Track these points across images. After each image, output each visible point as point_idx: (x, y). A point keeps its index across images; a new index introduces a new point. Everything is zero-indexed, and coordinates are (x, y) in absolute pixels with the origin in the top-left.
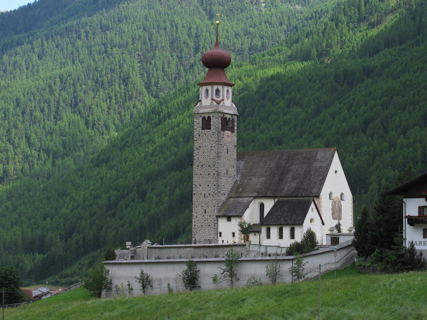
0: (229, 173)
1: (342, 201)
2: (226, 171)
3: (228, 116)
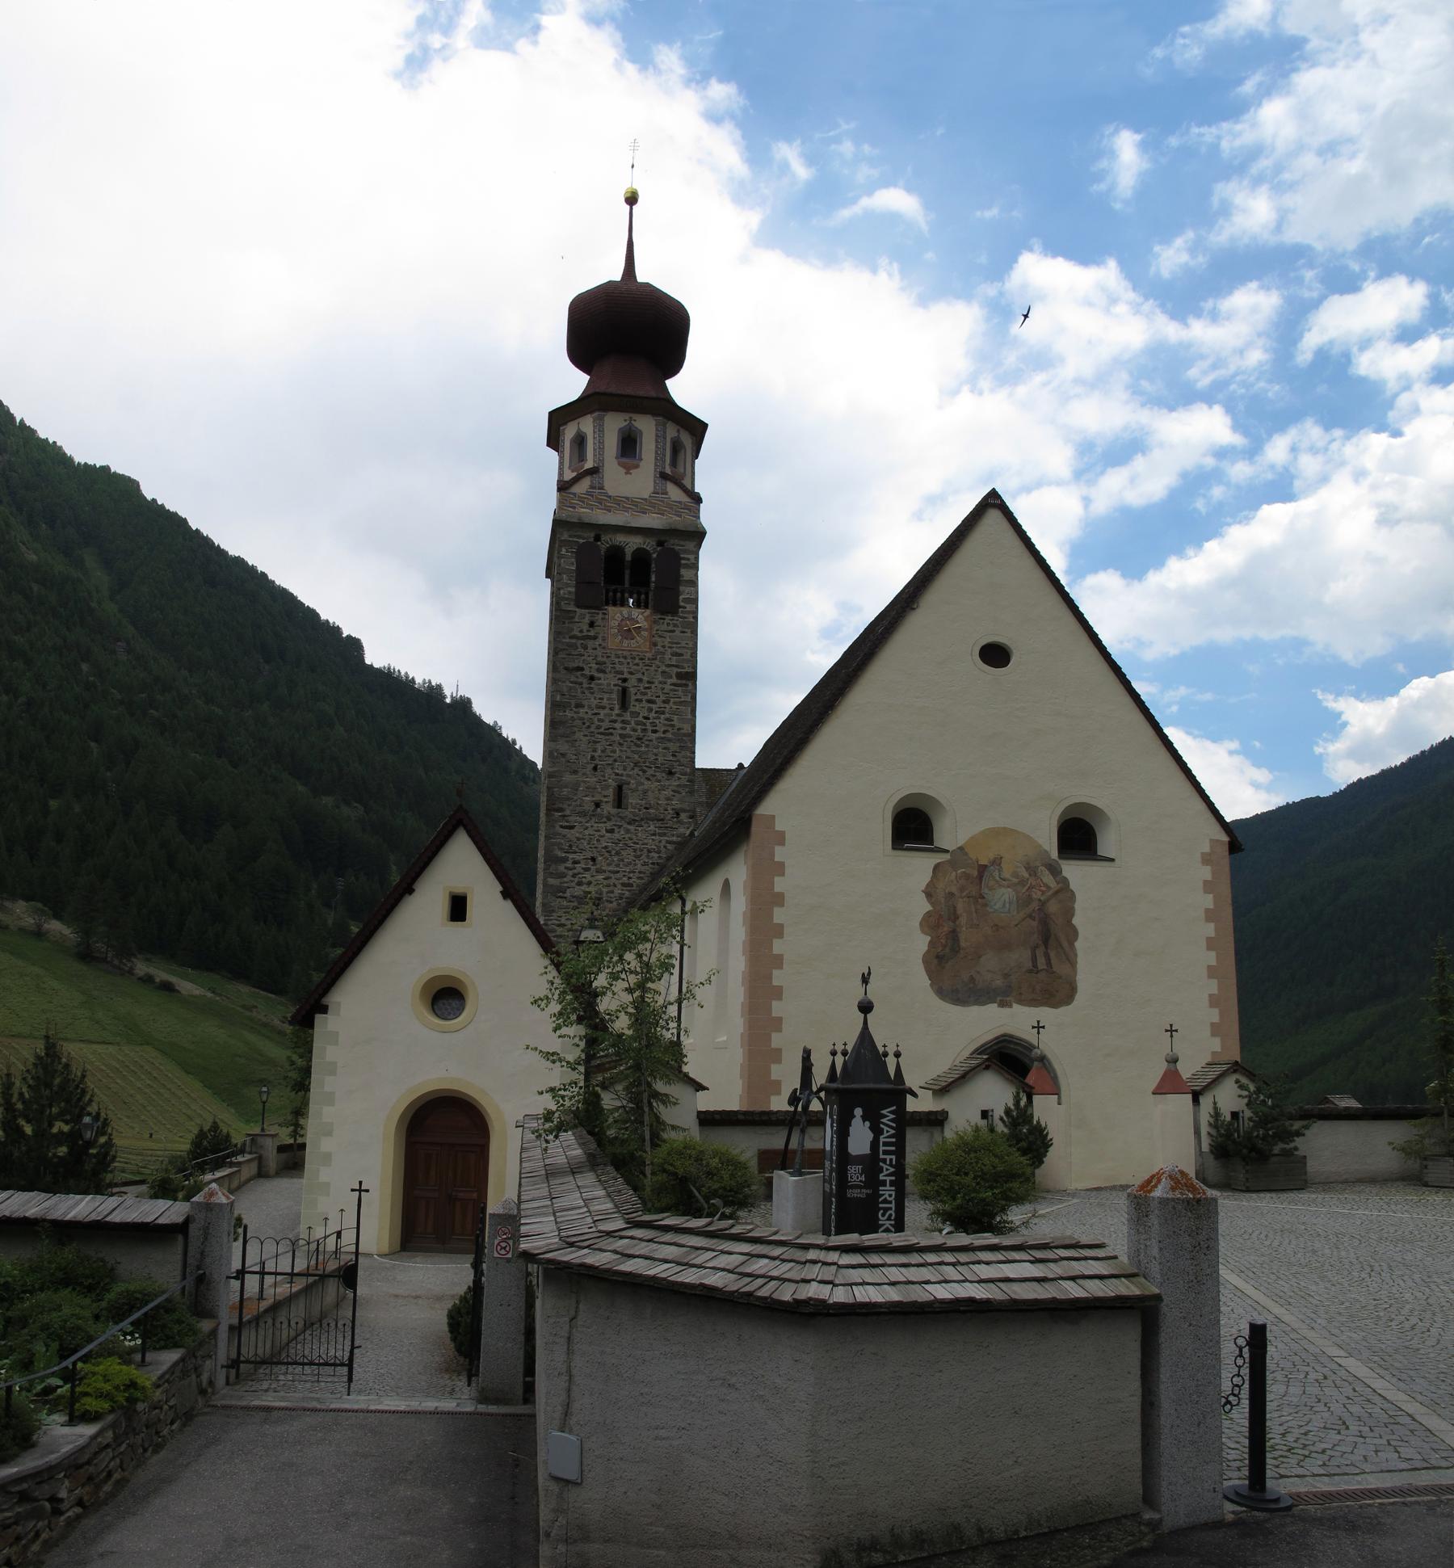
0: (632, 800)
1: (1076, 872)
2: (610, 792)
3: (632, 543)
